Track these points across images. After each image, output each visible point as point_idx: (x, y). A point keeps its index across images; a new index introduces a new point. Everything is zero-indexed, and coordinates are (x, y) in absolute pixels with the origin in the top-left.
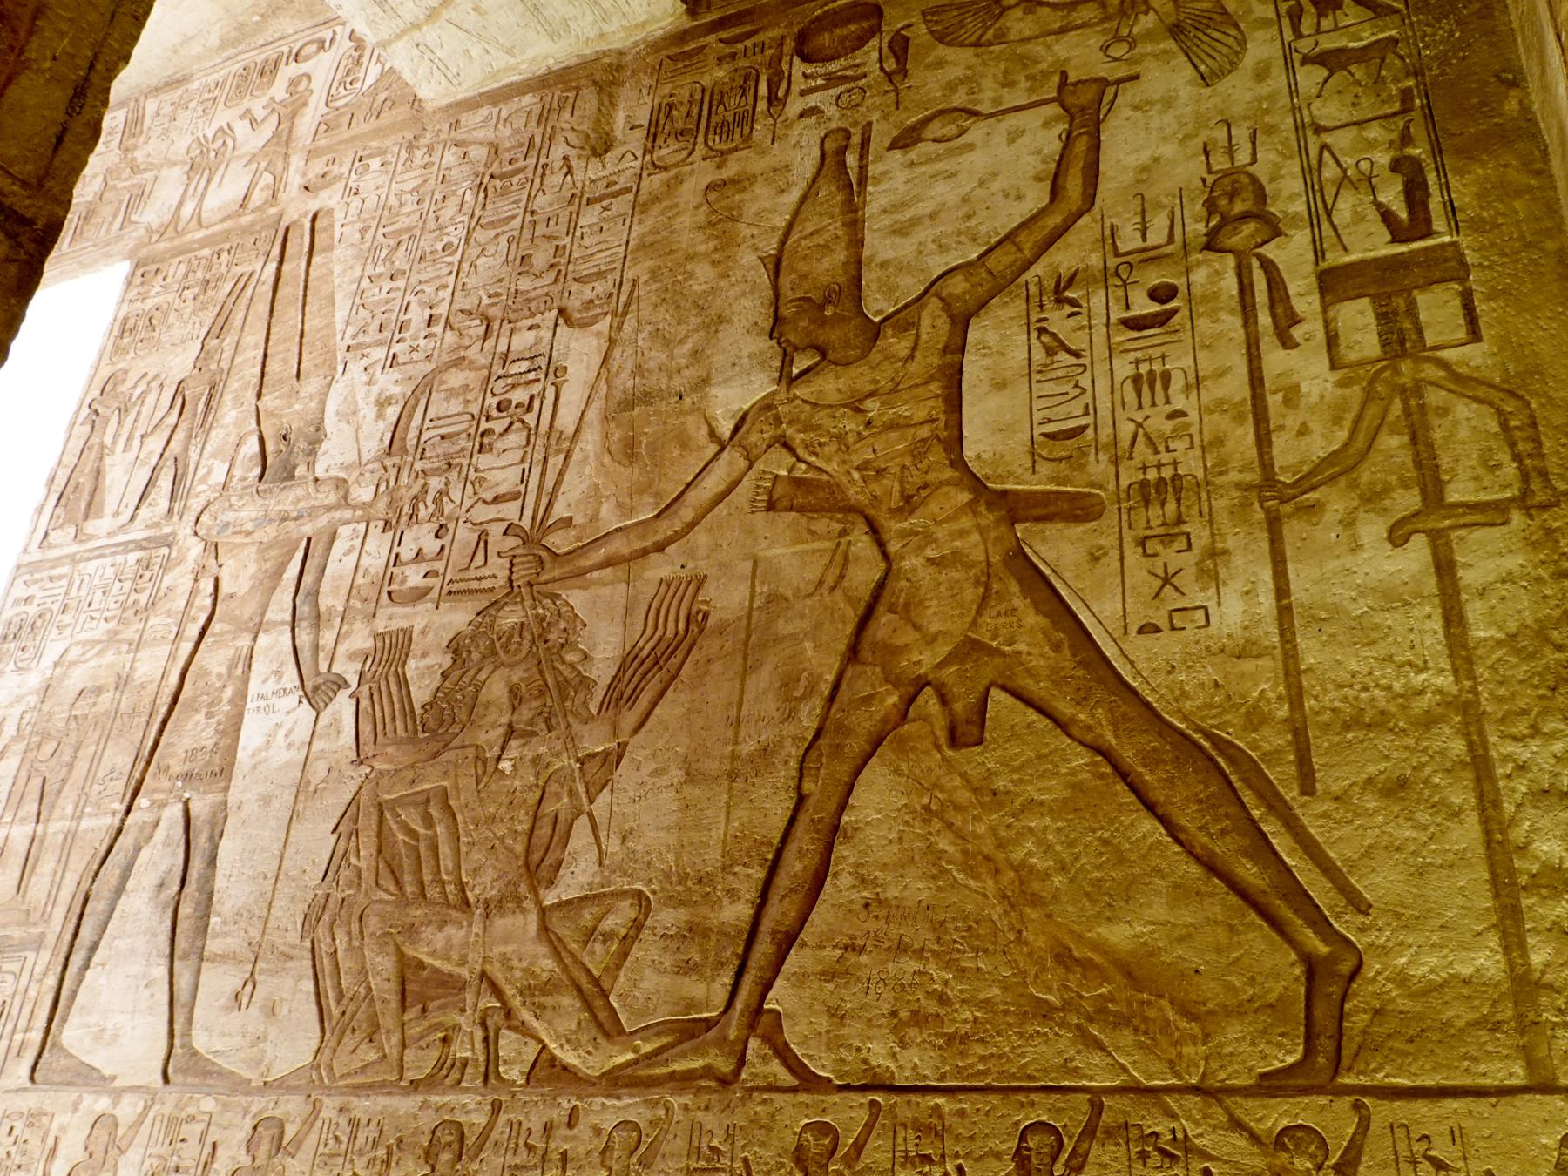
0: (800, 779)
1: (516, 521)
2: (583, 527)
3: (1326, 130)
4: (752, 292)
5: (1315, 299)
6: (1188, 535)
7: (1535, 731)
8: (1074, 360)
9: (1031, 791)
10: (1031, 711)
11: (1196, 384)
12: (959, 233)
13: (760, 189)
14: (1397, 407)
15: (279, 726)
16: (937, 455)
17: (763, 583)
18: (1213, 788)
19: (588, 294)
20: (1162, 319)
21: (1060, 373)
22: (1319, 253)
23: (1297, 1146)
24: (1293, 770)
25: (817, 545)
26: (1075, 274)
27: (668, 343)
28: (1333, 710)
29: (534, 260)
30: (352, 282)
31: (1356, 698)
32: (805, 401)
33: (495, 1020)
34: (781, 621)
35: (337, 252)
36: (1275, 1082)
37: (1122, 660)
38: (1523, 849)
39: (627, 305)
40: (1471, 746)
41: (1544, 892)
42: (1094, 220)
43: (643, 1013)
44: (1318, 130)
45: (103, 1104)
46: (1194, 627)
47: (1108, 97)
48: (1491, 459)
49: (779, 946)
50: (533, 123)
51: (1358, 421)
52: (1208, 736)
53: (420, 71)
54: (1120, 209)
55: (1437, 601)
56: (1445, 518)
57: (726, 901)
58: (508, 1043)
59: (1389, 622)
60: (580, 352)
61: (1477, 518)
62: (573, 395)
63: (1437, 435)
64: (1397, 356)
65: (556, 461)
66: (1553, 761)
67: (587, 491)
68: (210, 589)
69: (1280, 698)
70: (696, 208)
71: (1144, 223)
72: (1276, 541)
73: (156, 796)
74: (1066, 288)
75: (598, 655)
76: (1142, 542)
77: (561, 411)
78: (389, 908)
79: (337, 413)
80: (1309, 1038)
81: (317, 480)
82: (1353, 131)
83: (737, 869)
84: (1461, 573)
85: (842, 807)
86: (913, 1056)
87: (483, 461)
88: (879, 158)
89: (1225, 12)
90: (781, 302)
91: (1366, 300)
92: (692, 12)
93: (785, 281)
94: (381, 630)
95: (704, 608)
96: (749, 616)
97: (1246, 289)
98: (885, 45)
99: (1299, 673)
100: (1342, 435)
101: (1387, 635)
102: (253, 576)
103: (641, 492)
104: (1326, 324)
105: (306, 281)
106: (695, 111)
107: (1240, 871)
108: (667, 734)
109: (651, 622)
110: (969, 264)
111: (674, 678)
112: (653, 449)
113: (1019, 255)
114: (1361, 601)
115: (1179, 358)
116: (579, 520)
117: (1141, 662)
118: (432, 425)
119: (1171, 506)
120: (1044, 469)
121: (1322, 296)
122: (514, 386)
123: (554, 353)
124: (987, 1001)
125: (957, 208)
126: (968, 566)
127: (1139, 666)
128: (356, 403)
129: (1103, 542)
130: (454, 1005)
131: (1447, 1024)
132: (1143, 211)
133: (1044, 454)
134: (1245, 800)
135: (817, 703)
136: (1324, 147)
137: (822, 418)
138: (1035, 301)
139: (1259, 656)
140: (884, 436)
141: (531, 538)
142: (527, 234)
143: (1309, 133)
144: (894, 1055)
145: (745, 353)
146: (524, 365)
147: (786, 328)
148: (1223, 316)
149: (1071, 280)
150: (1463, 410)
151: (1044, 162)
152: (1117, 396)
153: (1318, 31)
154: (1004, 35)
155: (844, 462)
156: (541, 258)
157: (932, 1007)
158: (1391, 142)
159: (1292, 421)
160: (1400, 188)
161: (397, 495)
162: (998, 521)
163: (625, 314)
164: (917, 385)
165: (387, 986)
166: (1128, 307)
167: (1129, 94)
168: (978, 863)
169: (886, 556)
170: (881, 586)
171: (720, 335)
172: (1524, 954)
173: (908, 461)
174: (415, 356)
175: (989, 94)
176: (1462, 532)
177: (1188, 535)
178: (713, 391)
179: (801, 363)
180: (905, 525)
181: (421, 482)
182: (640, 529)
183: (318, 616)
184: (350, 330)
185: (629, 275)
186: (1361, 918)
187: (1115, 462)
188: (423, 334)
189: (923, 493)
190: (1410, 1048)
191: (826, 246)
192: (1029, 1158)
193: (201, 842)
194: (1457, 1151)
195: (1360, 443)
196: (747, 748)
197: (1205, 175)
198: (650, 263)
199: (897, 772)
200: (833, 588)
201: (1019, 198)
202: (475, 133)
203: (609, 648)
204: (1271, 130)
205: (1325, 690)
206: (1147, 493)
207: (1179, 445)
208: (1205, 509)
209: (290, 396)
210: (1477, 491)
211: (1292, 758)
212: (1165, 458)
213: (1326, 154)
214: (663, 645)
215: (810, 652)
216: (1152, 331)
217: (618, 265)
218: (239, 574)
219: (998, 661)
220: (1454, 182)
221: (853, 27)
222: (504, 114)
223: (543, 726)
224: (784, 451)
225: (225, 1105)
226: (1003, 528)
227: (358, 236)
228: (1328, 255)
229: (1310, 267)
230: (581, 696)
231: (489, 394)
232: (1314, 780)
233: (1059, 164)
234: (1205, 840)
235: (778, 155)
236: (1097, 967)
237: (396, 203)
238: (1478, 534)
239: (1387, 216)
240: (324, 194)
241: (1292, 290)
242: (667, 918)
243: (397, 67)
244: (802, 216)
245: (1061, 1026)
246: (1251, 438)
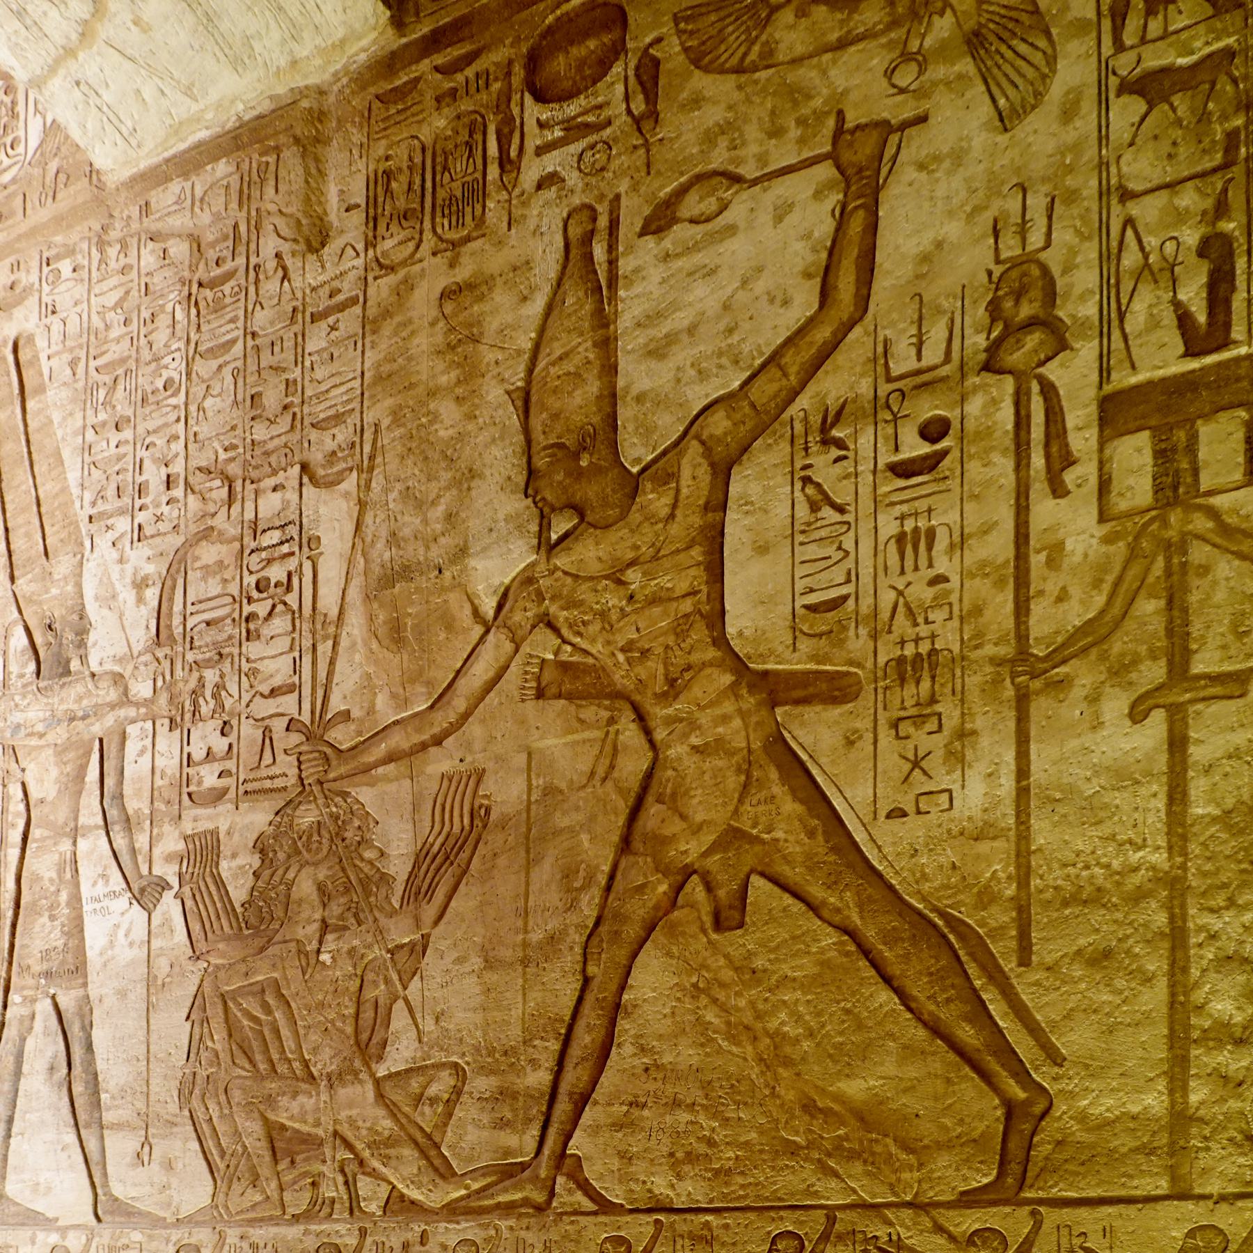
0: (585, 963)
1: (296, 716)
2: (361, 721)
3: (1135, 195)
4: (502, 438)
5: (1093, 434)
6: (940, 715)
7: (1231, 903)
8: (837, 517)
9: (786, 969)
10: (786, 895)
11: (960, 543)
12: (720, 354)
13: (501, 297)
15: (117, 926)
16: (699, 633)
17: (538, 776)
18: (942, 961)
19: (330, 445)
20: (929, 464)
21: (823, 533)
22: (1104, 372)
23: (984, 1243)
24: (1013, 944)
25: (587, 734)
27: (420, 505)
28: (1056, 888)
29: (265, 401)
30: (75, 434)
31: (1077, 876)
32: (566, 573)
33: (351, 1168)
34: (558, 814)
35: (50, 393)
36: (971, 1198)
37: (870, 845)
39: (372, 458)
40: (1172, 918)
41: (1211, 1044)
42: (867, 333)
43: (470, 1160)
44: (1126, 195)
45: (54, 1238)
48: (1242, 624)
49: (576, 1104)
50: (234, 205)
51: (1117, 584)
52: (942, 915)
53: (89, 126)
54: (895, 316)
55: (1164, 779)
56: (1186, 691)
57: (529, 1069)
58: (364, 1185)
59: (1117, 801)
60: (330, 514)
61: (1217, 690)
62: (331, 570)
63: (1194, 598)
64: (1168, 504)
65: (325, 648)
66: (1241, 930)
67: (360, 680)
68: (20, 795)
69: (1009, 877)
70: (433, 324)
71: (920, 335)
72: (1022, 719)
73: (25, 993)
74: (833, 425)
75: (393, 851)
76: (895, 725)
77: (322, 591)
78: (248, 1083)
79: (97, 598)
80: (1002, 1164)
81: (93, 675)
82: (1164, 194)
83: (536, 1042)
84: (1191, 749)
85: (622, 988)
86: (688, 1186)
87: (254, 649)
88: (630, 249)
89: (1036, 11)
90: (534, 450)
91: (1147, 433)
92: (398, 23)
93: (536, 423)
94: (189, 832)
95: (486, 802)
96: (528, 810)
97: (1022, 422)
98: (631, 73)
99: (1029, 853)
100: (1100, 600)
101: (1114, 814)
102: (57, 781)
103: (413, 681)
104: (1101, 463)
105: (27, 434)
106: (418, 181)
107: (959, 1033)
108: (464, 926)
109: (437, 818)
110: (731, 396)
111: (465, 872)
112: (419, 632)
113: (784, 382)
114: (1095, 781)
115: (945, 512)
116: (356, 713)
117: (886, 845)
118: (194, 609)
119: (926, 684)
120: (805, 645)
121: (1101, 430)
122: (269, 561)
123: (305, 520)
124: (747, 1143)
125: (718, 318)
126: (730, 753)
127: (886, 850)
128: (112, 584)
129: (858, 725)
130: (316, 1157)
131: (1115, 1150)
132: (921, 318)
133: (805, 629)
134: (970, 972)
135: (596, 893)
136: (1129, 222)
137: (583, 591)
139: (994, 838)
140: (647, 612)
141: (314, 732)
142: (252, 367)
143: (1114, 201)
144: (672, 1186)
145: (501, 516)
146: (275, 536)
147: (542, 483)
148: (996, 457)
149: (839, 414)
150: (1225, 568)
151: (814, 250)
153: (1143, 41)
154: (771, 53)
155: (608, 643)
156: (272, 398)
157: (702, 1148)
158: (1204, 213)
159: (1052, 588)
160: (1204, 279)
161: (176, 691)
162: (759, 704)
163: (371, 469)
164: (678, 551)
165: (258, 1144)
166: (897, 449)
167: (916, 146)
168: (738, 1032)
170: (649, 775)
171: (473, 493)
172: (1185, 1095)
174: (162, 527)
175: (753, 149)
176: (1200, 706)
177: (940, 715)
178: (472, 562)
179: (560, 526)
180: (670, 711)
181: (196, 675)
182: (417, 721)
183: (128, 820)
184: (88, 497)
185: (369, 418)
186: (1056, 1069)
187: (874, 636)
188: (165, 499)
189: (687, 676)
190: (1082, 1169)
191: (577, 375)
193: (75, 1031)
195: (1116, 610)
196: (536, 936)
197: (992, 266)
198: (389, 402)
199: (669, 954)
200: (604, 780)
201: (786, 303)
202: (170, 220)
203: (402, 844)
204: (1072, 197)
205: (1050, 869)
206: (905, 670)
207: (938, 616)
208: (958, 687)
209: (44, 579)
210: (1222, 661)
211: (1014, 933)
212: (923, 630)
213: (1129, 233)
214: (451, 841)
215: (586, 844)
216: (920, 479)
217: (356, 404)
218: (44, 777)
219: (758, 848)
221: (592, 44)
222: (199, 192)
223: (353, 921)
224: (548, 631)
225: (150, 1236)
226: (764, 712)
227: (69, 372)
228: (1114, 376)
229: (1092, 392)
230: (383, 892)
231: (246, 573)
232: (1031, 952)
233: (831, 254)
234: (933, 1007)
235: (519, 244)
236: (836, 1114)
237: (101, 326)
238: (1216, 707)
239: (1184, 319)
240: (18, 313)
241: (1070, 424)
242: (481, 1084)
243: (60, 120)
244: (549, 333)
245: (805, 1160)
246: (1010, 606)
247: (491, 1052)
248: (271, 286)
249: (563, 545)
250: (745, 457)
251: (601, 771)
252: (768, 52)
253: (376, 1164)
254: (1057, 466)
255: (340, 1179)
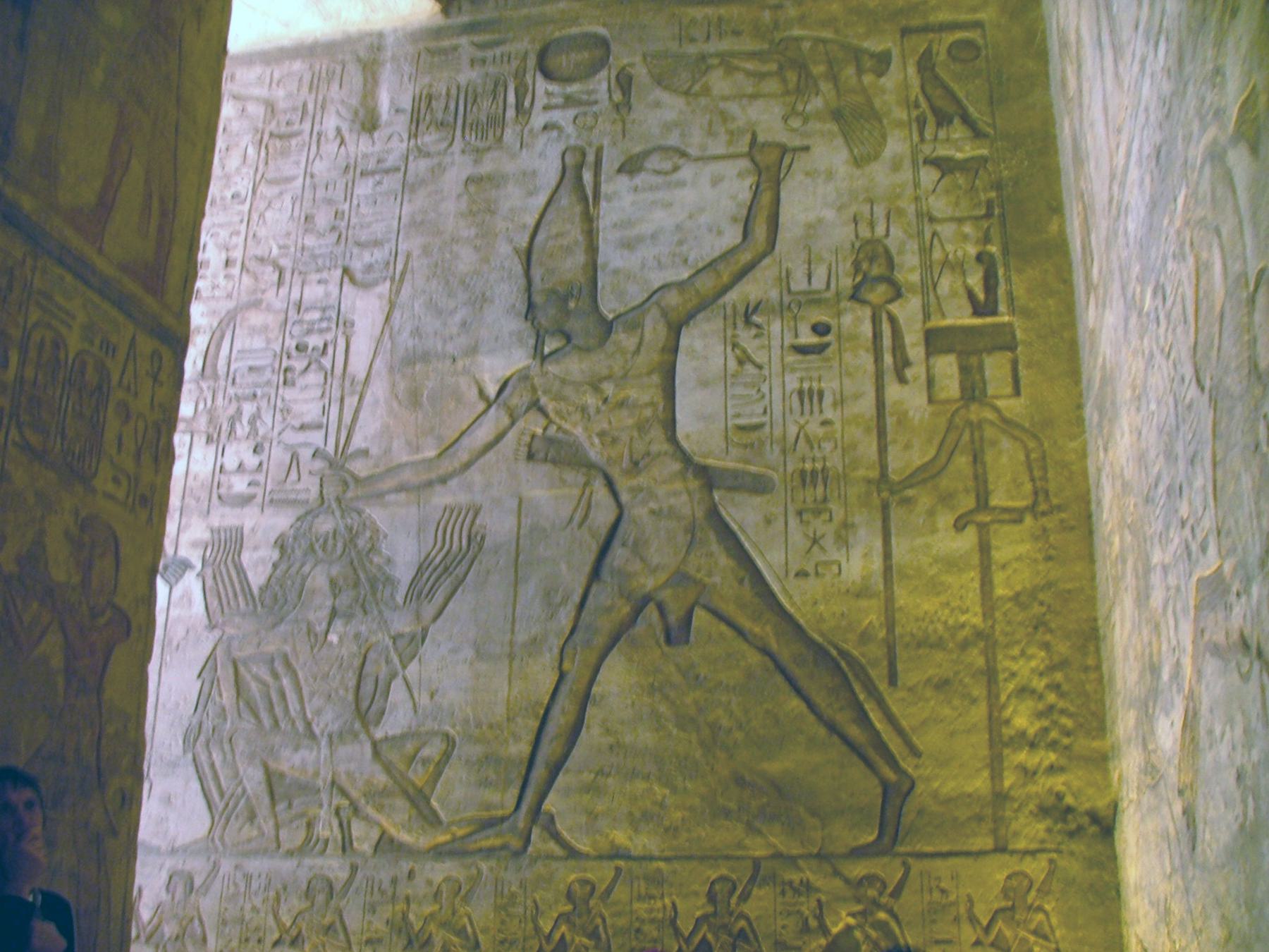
11: (840, 402)
12: (674, 255)
14: (966, 437)
16: (657, 433)
18: (833, 677)
19: (367, 258)
20: (820, 349)
22: (927, 316)
26: (759, 303)
27: (439, 312)
38: (1007, 722)
39: (403, 274)
44: (932, 219)
46: (833, 574)
47: (786, 161)
50: (305, 89)
58: (357, 829)
63: (989, 458)
65: (351, 402)
70: (459, 196)
92: (446, 11)
93: (537, 273)
97: (877, 336)
106: (452, 106)
119: (820, 490)
121: (927, 349)
122: (309, 332)
137: (569, 391)
138: (730, 321)
143: (926, 220)
148: (862, 352)
152: (787, 403)
166: (796, 336)
167: (802, 162)
168: (684, 722)
169: (619, 505)
173: (635, 434)
174: (217, 293)
187: (784, 451)
196: (521, 637)
204: (901, 212)
206: (806, 478)
207: (827, 446)
212: (818, 455)
214: (451, 557)
220: (1014, 278)
222: (276, 76)
229: (918, 326)
230: (387, 593)
235: (527, 160)
239: (971, 295)
244: (548, 217)
247: (479, 725)
248: (331, 147)
249: (555, 356)
250: (692, 323)
251: (578, 518)
252: (706, 91)
253: (370, 810)
254: (900, 365)
255: (335, 823)
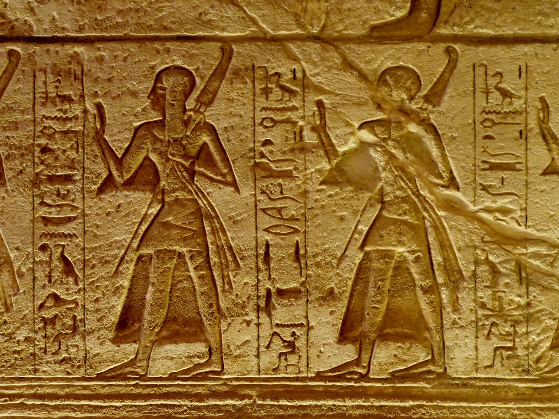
23: (396, 82)
36: (384, 33)
192: (164, 96)
194: (521, 83)
